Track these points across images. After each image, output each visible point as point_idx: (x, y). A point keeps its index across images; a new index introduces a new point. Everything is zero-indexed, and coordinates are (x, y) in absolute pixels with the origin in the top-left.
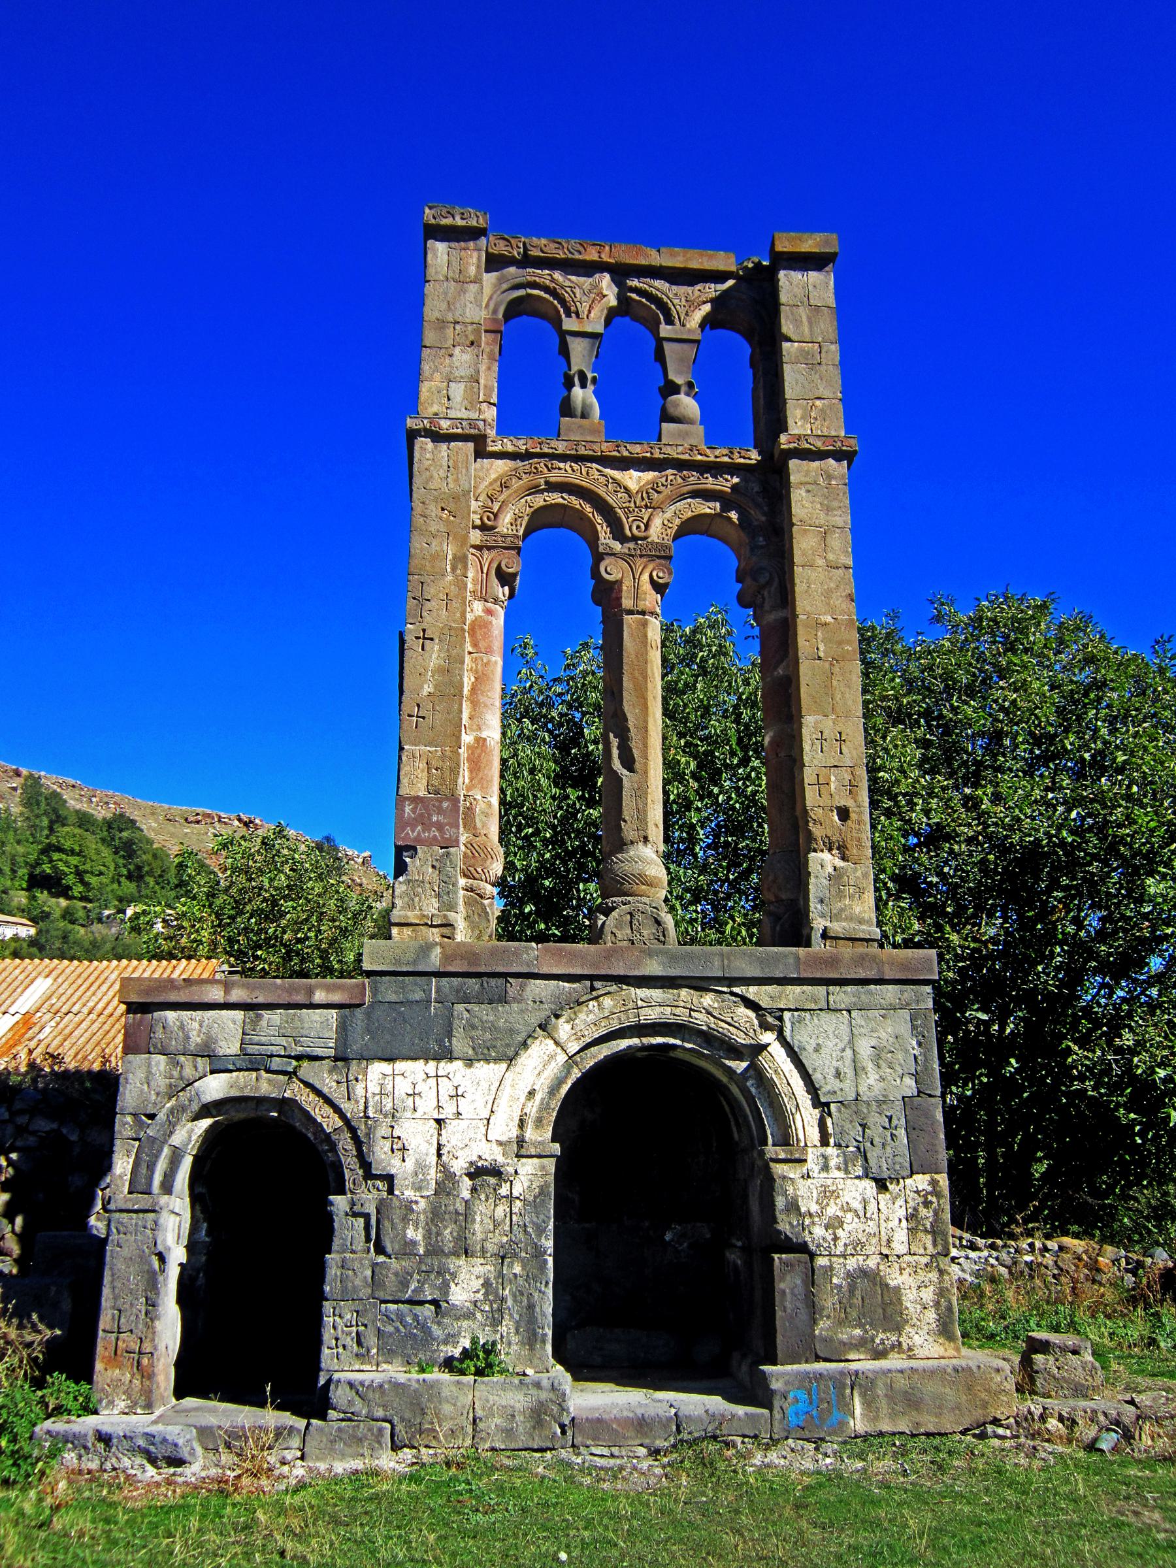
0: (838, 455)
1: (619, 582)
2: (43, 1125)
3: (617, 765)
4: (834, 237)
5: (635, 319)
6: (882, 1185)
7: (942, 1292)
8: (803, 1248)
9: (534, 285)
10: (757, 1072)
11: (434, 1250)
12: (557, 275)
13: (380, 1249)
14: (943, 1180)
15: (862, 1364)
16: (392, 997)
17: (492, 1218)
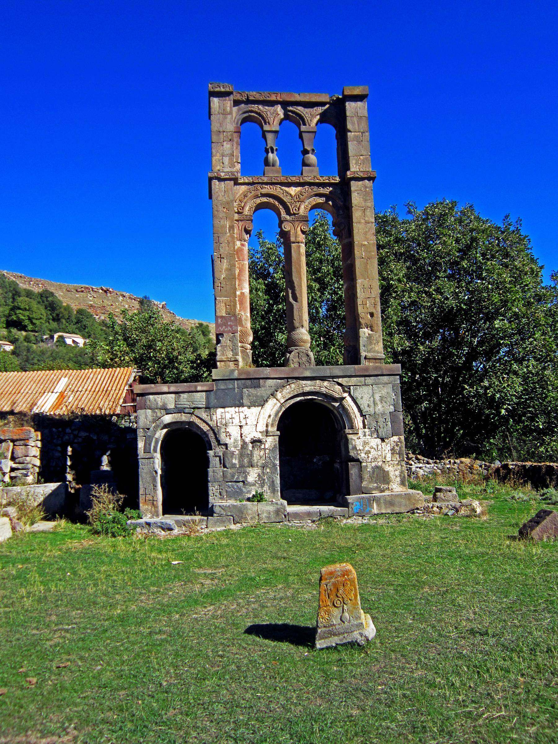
0: (369, 179)
1: (289, 231)
2: (83, 434)
3: (291, 300)
4: (367, 88)
5: (291, 121)
6: (383, 440)
7: (402, 472)
8: (358, 460)
9: (252, 111)
10: (342, 406)
11: (242, 466)
12: (260, 107)
13: (225, 466)
14: (402, 438)
15: (377, 494)
16: (223, 387)
17: (259, 455)
